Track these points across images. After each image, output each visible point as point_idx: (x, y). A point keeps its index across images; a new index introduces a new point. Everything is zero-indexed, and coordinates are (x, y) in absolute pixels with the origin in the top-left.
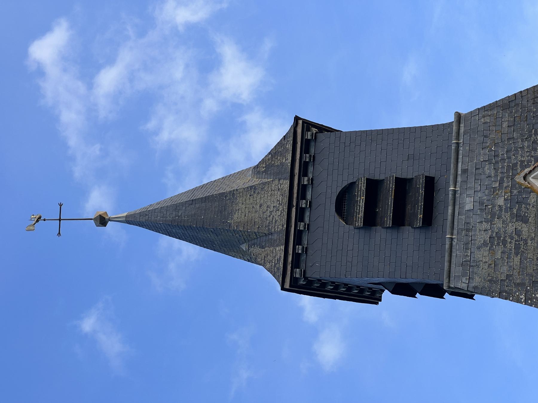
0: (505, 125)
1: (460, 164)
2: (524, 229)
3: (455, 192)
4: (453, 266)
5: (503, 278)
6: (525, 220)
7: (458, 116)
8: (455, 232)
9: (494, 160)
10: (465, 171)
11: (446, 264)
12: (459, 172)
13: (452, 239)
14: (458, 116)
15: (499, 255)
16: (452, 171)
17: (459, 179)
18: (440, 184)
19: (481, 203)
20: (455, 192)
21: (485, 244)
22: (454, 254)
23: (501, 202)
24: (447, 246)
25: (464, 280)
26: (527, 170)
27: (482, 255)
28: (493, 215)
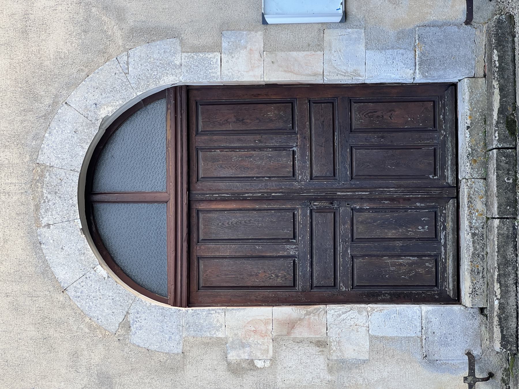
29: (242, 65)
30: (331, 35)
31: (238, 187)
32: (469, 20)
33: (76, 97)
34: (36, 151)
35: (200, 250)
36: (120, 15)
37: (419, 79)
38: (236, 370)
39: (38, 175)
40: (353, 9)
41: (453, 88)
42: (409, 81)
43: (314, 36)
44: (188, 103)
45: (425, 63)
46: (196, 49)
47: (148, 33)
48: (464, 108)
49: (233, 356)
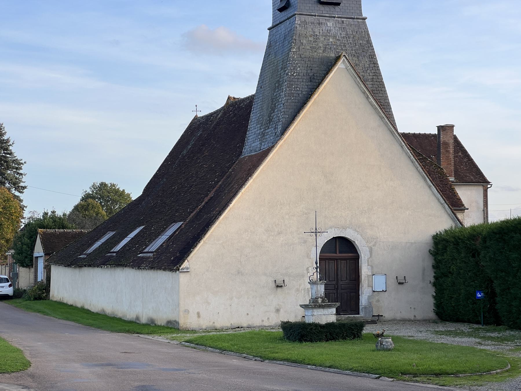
0: (361, 42)
1: (345, 19)
2: (321, 51)
3: (335, 17)
4: (304, 16)
5: (302, 41)
6: (324, 51)
7: (365, 19)
8: (318, 17)
9: (347, 36)
10: (343, 22)
11: (305, 13)
12: (343, 19)
13: (315, 16)
14: (365, 19)
15: (310, 39)
16: (343, 16)
17: (340, 19)
18: (337, 8)
19: (330, 31)
20: (335, 17)
21: (314, 32)
22: (309, 17)
23: (331, 40)
24: (312, 14)
25: (299, 22)
26: (347, 57)
27: (309, 31)
28: (326, 36)
29: (365, 270)
30: (371, 288)
31: (339, 269)
32: (373, 316)
33: (359, 236)
34: (349, 228)
35: (327, 261)
36: (374, 245)
37: (361, 308)
38: (307, 269)
39: (344, 228)
40: (376, 293)
41: (359, 314)
42: (360, 304)
43: (370, 286)
44: (356, 258)
45: (365, 308)
46: (368, 261)
47: (371, 251)
48: (357, 316)
49: (310, 268)
